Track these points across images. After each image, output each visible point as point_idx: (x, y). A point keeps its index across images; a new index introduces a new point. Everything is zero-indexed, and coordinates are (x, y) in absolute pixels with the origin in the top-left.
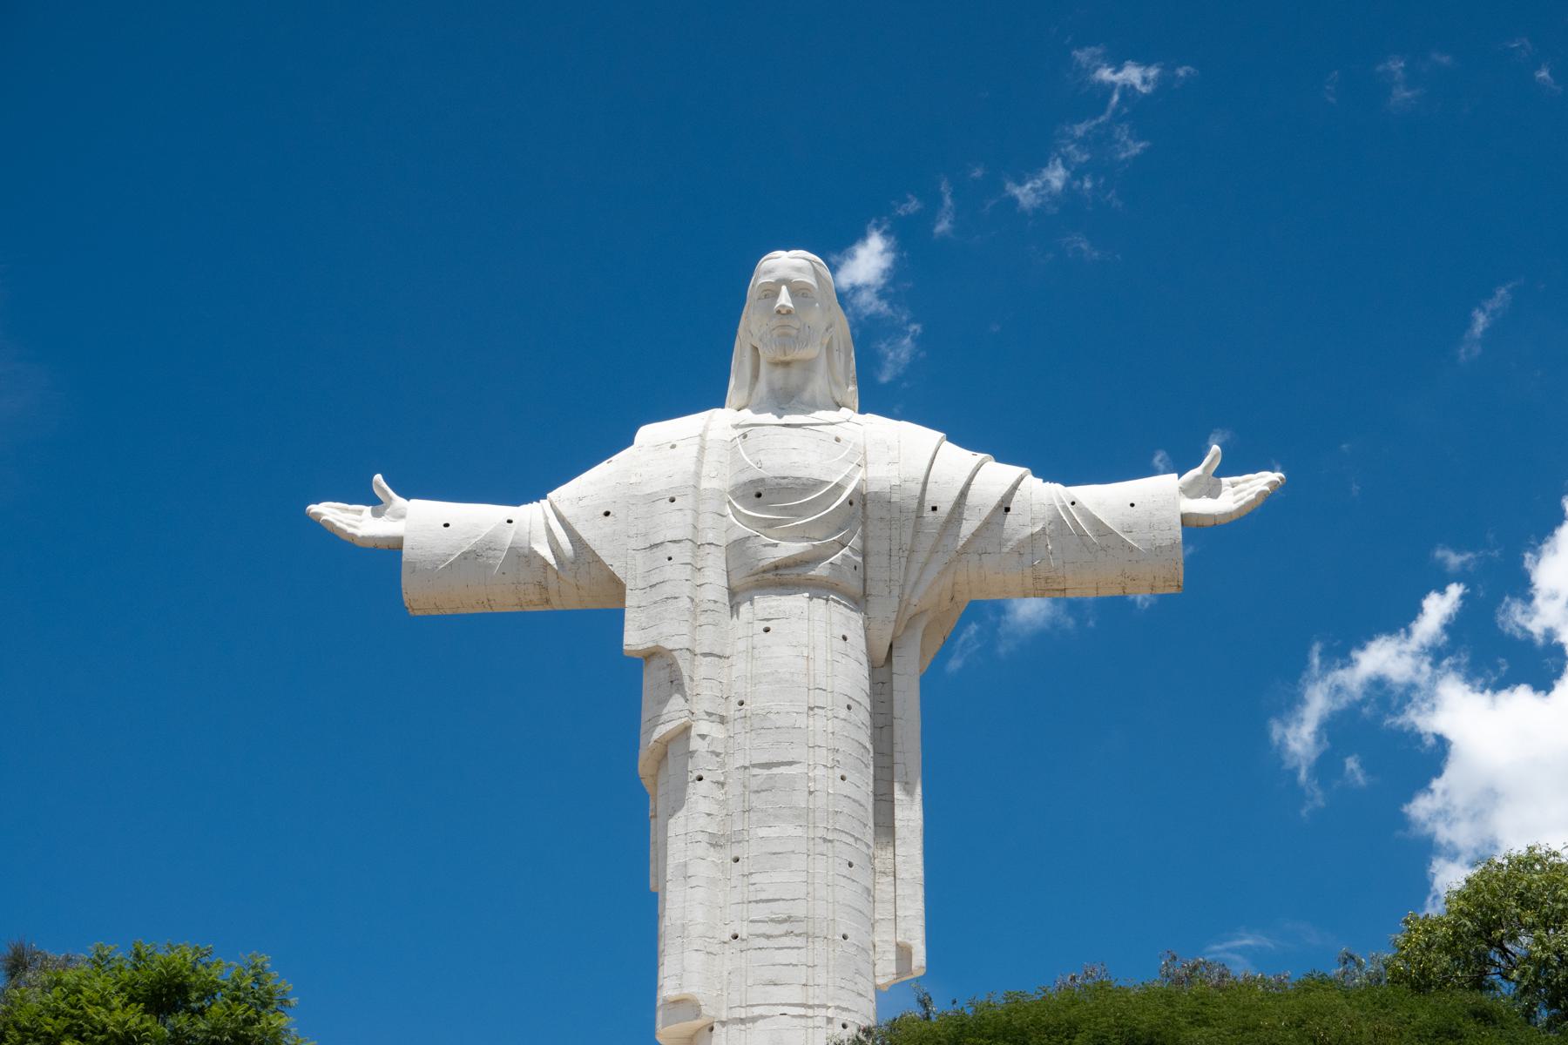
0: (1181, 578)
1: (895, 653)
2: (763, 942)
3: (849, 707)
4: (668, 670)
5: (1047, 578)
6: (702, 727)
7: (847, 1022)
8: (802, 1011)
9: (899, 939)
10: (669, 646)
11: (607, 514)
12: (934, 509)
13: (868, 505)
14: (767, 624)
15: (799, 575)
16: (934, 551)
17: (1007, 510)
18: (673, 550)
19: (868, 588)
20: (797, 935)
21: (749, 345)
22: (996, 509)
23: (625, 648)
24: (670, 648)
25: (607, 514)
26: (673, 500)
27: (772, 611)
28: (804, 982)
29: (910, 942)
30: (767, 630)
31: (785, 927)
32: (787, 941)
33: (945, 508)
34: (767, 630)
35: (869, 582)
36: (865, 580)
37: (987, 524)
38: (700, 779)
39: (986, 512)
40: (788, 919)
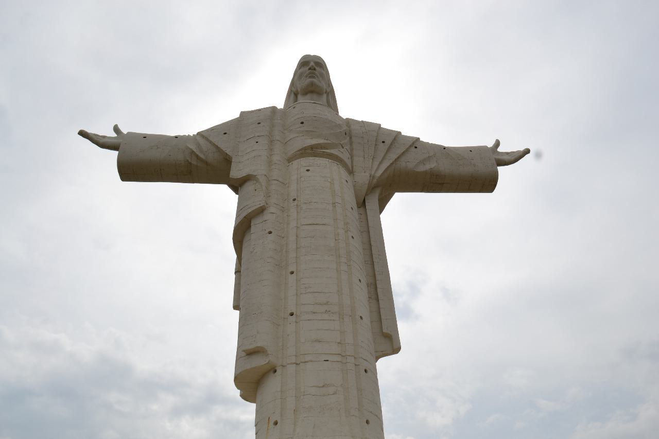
1: (366, 201)
3: (352, 208)
4: (254, 186)
5: (437, 176)
6: (272, 210)
7: (367, 369)
8: (339, 358)
9: (384, 331)
10: (254, 174)
11: (225, 134)
12: (383, 142)
13: (353, 138)
14: (308, 168)
15: (324, 152)
16: (384, 158)
18: (259, 140)
21: (293, 93)
22: (411, 146)
23: (231, 177)
25: (225, 134)
26: (259, 123)
28: (339, 341)
29: (389, 332)
30: (308, 170)
33: (388, 142)
34: (308, 170)
35: (354, 167)
36: (352, 167)
37: (407, 150)
38: (270, 233)
40: (327, 303)
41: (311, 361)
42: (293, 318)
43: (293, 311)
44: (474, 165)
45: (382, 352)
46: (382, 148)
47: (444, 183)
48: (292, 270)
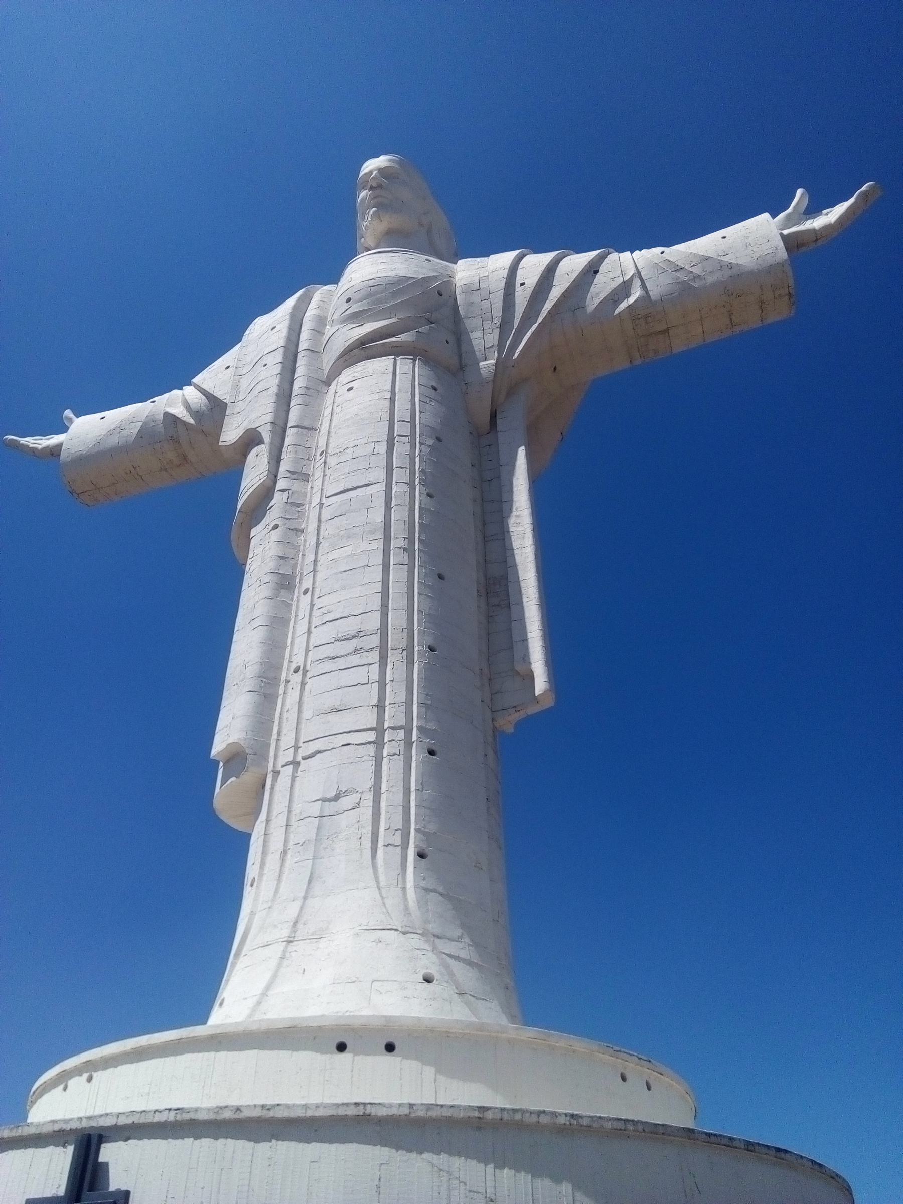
0: (791, 282)
2: (328, 666)
5: (646, 316)
10: (254, 427)
14: (350, 385)
17: (596, 272)
19: (463, 361)
20: (367, 651)
24: (256, 427)
27: (356, 374)
31: (353, 644)
32: (355, 660)
34: (350, 389)
36: (460, 356)
38: (276, 527)
39: (574, 276)
41: (319, 752)
42: (297, 678)
43: (299, 664)
44: (730, 266)
45: (515, 707)
46: (522, 298)
47: (668, 329)
48: (308, 587)
